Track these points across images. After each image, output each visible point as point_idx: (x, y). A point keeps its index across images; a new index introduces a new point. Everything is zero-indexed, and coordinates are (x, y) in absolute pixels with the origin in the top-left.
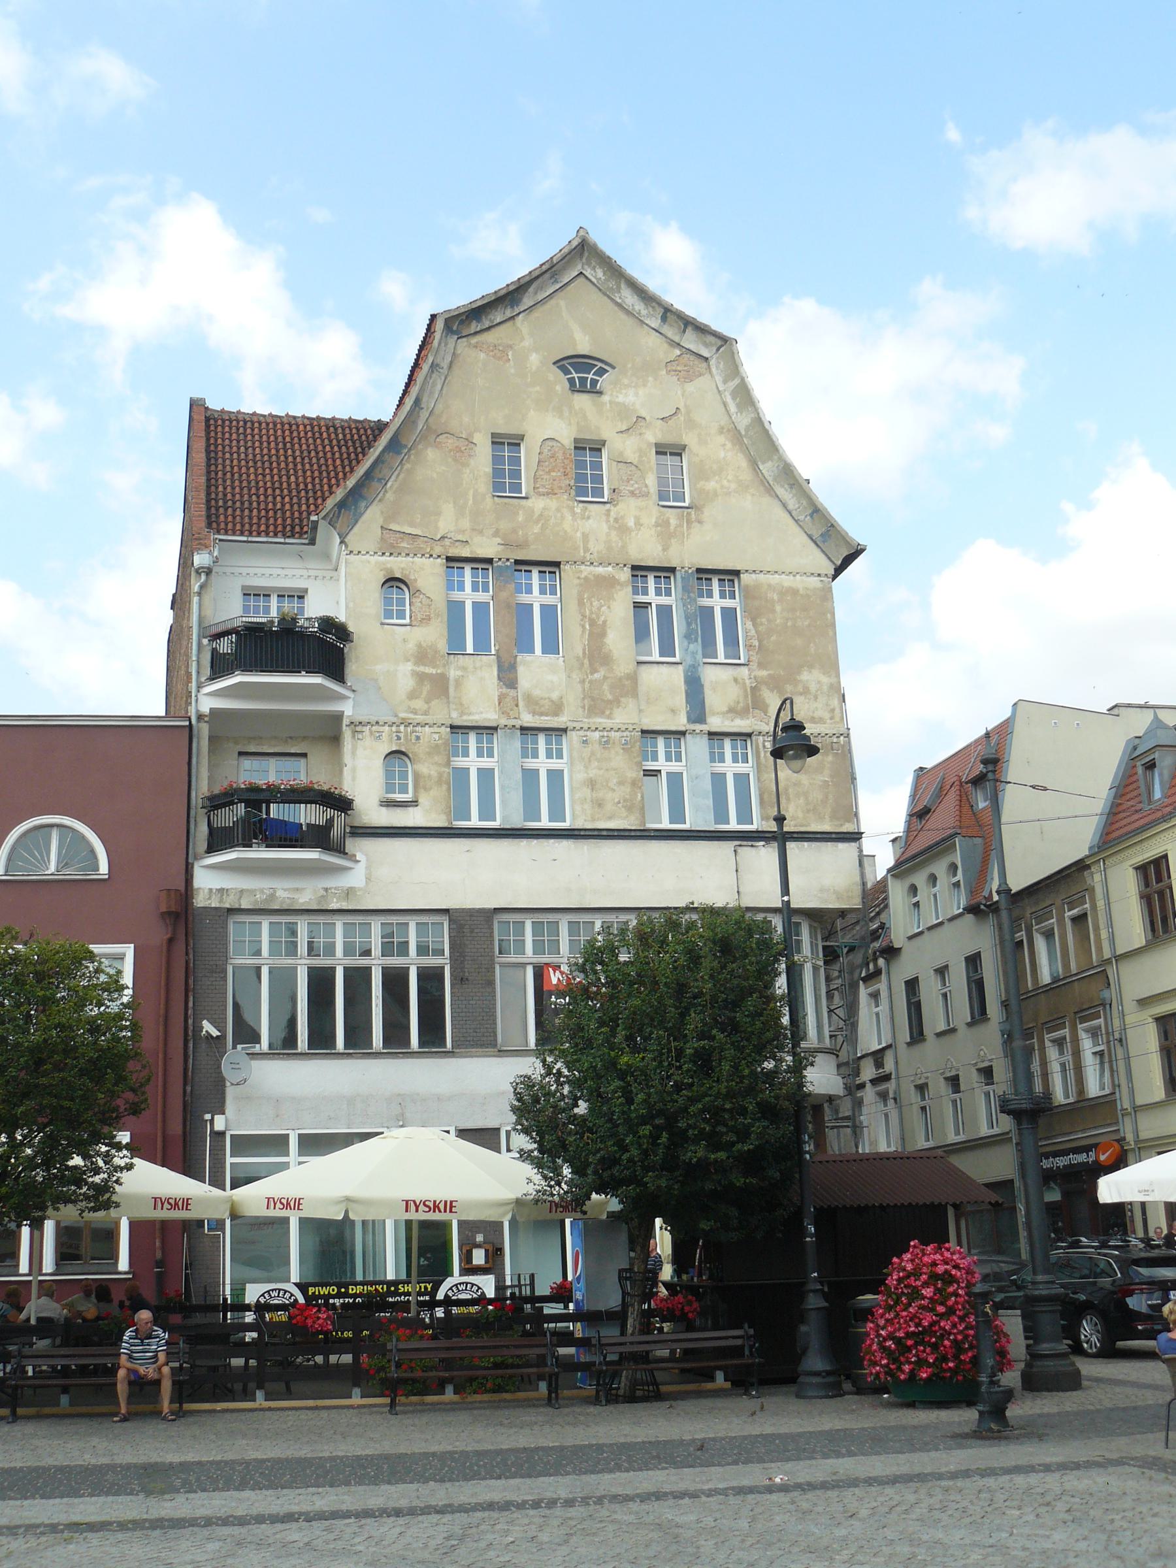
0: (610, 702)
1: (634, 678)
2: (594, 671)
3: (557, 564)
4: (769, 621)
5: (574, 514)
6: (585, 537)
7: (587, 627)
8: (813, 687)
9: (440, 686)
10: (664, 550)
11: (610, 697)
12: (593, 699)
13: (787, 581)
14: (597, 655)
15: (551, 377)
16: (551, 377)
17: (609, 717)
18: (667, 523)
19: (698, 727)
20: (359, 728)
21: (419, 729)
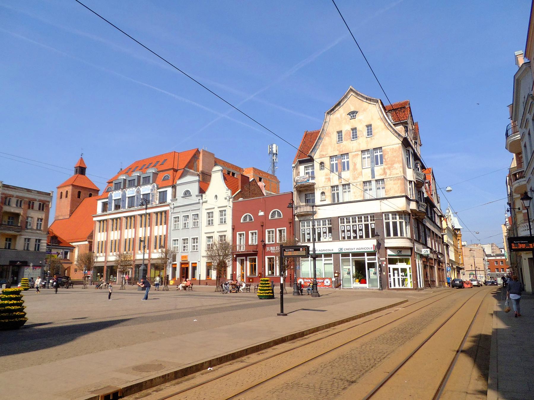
0: (357, 177)
1: (362, 172)
2: (354, 172)
3: (348, 153)
4: (388, 156)
5: (351, 143)
6: (353, 147)
7: (353, 164)
8: (396, 168)
9: (329, 179)
10: (367, 146)
11: (357, 176)
12: (354, 177)
13: (392, 147)
14: (355, 169)
15: (347, 117)
16: (347, 117)
17: (357, 180)
18: (368, 141)
19: (373, 179)
20: (317, 189)
21: (326, 187)
